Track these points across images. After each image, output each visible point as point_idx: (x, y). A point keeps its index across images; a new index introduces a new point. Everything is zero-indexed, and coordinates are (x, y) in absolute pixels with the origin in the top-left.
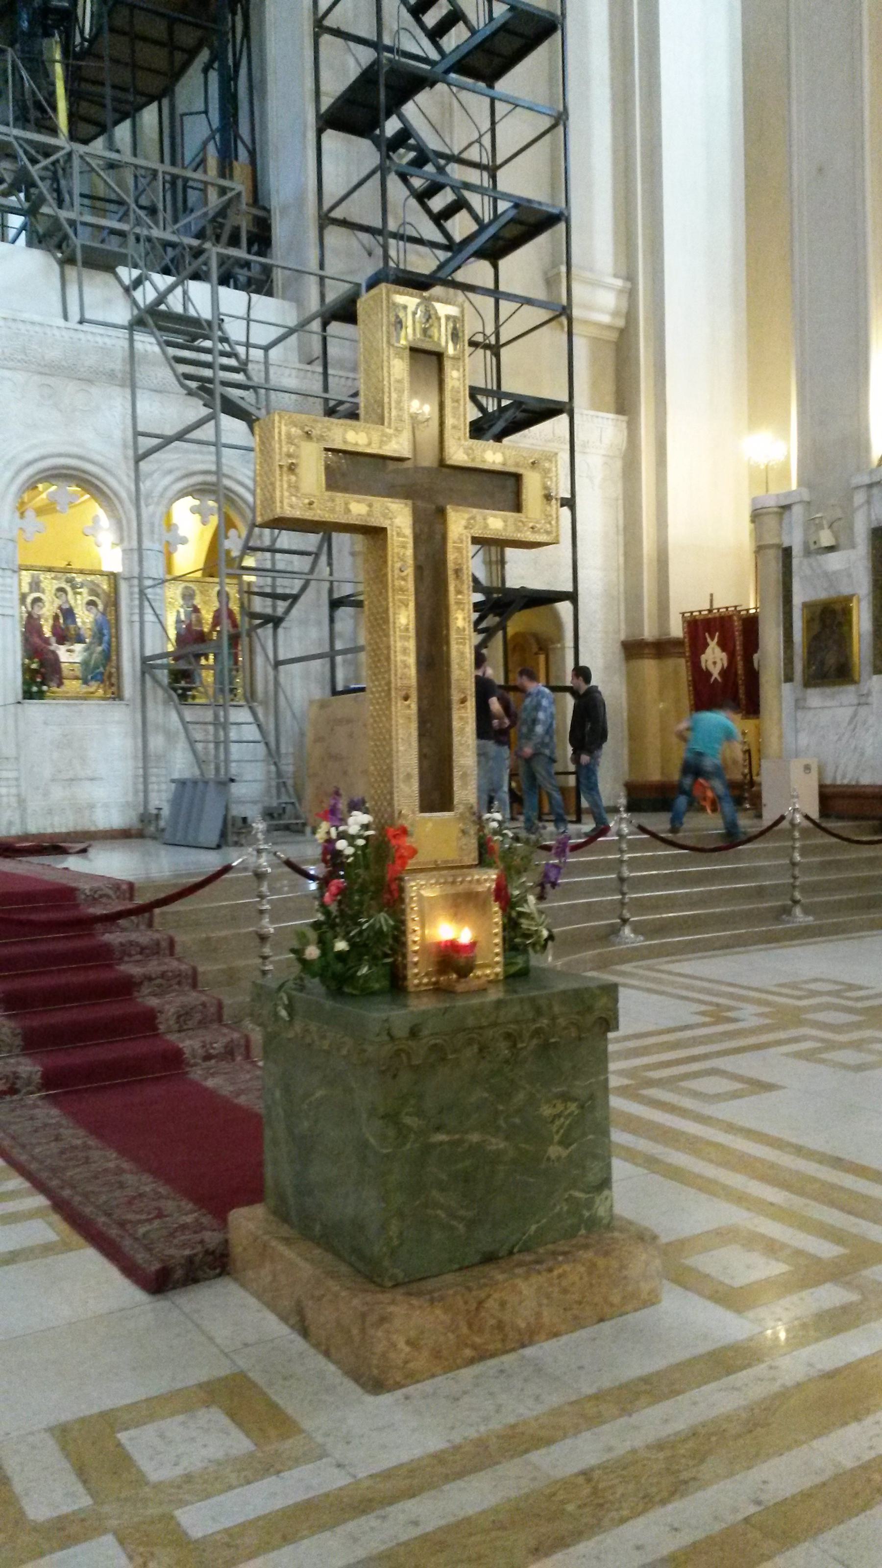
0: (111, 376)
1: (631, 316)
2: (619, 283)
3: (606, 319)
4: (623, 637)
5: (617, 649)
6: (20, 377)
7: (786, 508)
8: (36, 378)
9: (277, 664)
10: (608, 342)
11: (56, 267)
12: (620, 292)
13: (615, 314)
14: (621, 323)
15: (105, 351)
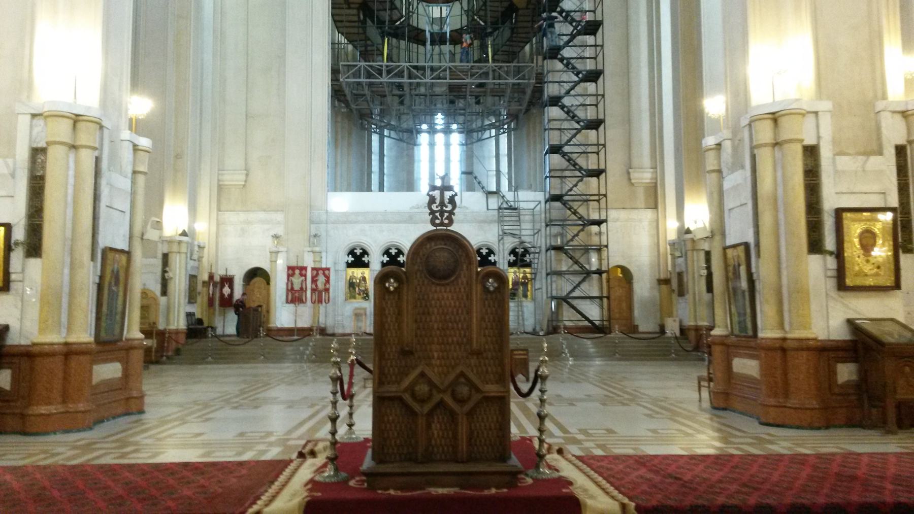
0: (495, 221)
1: (656, 178)
2: (652, 170)
3: (648, 181)
4: (657, 278)
5: (656, 282)
6: (474, 224)
7: (674, 243)
8: (478, 224)
9: (535, 290)
10: (651, 187)
11: (485, 195)
12: (652, 173)
13: (652, 179)
14: (655, 181)
15: (494, 215)
